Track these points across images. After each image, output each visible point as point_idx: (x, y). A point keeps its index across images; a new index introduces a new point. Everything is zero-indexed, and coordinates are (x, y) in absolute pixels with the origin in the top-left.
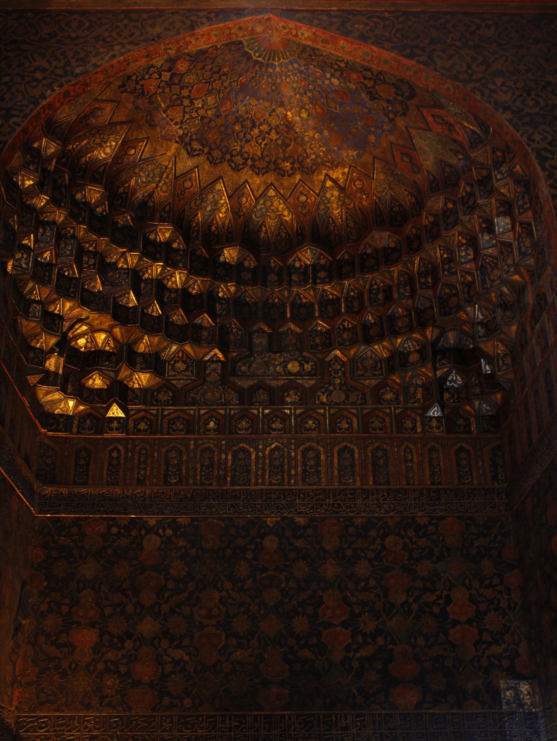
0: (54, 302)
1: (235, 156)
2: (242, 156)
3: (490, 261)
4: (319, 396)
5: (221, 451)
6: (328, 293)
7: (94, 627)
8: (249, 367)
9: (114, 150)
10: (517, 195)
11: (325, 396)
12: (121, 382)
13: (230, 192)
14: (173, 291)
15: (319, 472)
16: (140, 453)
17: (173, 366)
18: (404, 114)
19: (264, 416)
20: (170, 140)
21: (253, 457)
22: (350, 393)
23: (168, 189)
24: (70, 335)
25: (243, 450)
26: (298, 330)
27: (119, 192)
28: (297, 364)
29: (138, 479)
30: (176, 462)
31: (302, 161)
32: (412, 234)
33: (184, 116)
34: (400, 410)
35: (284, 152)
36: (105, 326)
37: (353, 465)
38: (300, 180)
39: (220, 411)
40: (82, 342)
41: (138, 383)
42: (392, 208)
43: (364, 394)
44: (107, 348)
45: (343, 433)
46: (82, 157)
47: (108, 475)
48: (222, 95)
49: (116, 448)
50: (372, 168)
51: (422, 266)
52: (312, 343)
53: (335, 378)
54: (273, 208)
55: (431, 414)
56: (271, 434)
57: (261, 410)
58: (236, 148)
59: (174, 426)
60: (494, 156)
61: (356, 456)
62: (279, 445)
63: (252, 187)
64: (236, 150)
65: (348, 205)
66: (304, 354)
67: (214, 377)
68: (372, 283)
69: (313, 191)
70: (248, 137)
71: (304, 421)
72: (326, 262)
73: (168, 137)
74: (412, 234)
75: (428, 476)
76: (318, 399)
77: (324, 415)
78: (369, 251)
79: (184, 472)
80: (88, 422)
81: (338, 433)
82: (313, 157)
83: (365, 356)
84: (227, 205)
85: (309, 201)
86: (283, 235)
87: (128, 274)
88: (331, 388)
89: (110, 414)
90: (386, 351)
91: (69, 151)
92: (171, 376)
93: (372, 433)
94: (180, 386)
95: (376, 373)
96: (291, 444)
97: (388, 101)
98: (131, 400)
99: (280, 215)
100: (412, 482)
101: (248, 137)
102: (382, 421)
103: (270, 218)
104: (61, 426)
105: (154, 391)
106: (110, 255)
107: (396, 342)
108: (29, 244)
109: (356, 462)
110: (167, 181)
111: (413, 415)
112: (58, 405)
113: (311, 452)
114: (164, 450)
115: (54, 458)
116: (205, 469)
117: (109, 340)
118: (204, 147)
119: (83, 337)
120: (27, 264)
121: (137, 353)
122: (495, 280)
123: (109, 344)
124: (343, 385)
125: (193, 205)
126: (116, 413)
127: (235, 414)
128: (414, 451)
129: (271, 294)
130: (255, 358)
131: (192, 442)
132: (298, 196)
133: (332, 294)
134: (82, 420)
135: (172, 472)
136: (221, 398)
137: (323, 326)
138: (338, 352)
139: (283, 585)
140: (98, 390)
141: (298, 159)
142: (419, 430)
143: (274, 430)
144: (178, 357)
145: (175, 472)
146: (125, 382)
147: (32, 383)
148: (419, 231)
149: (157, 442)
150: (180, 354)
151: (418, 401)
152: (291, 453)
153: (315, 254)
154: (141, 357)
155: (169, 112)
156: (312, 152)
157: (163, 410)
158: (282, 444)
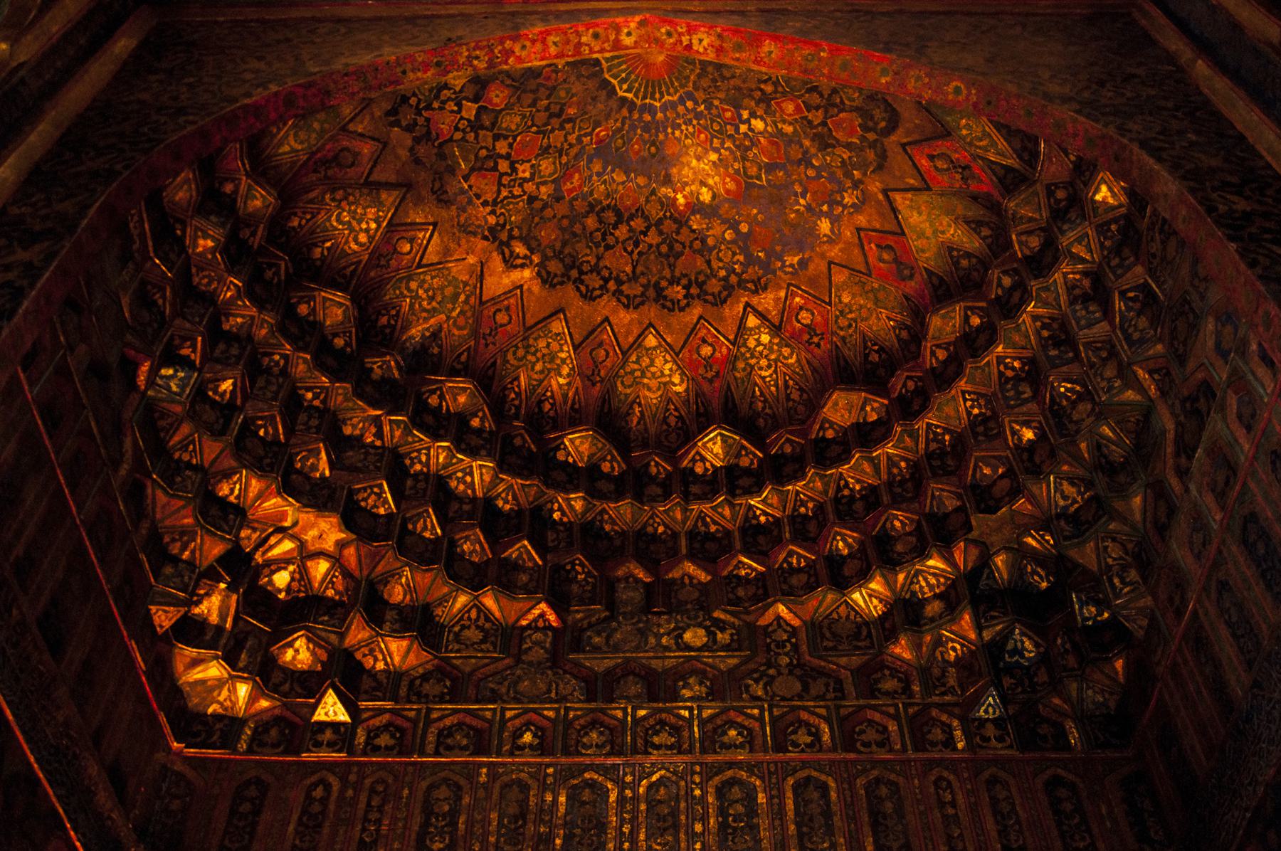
0: (227, 475)
1: (586, 273)
2: (599, 274)
3: (1067, 390)
4: (747, 687)
5: (544, 787)
6: (758, 512)
8: (608, 638)
9: (373, 238)
10: (1105, 253)
11: (760, 686)
12: (349, 654)
13: (578, 339)
14: (467, 501)
15: (753, 828)
16: (372, 791)
17: (457, 635)
18: (880, 167)
19: (636, 721)
20: (474, 234)
21: (613, 797)
22: (810, 680)
23: (467, 323)
24: (258, 558)
25: (592, 785)
26: (703, 577)
27: (380, 324)
28: (702, 632)
29: (361, 841)
30: (447, 808)
31: (704, 283)
32: (907, 391)
33: (499, 192)
34: (916, 708)
35: (672, 267)
36: (329, 544)
37: (827, 814)
38: (701, 317)
39: (546, 712)
40: (282, 579)
41: (384, 659)
42: (867, 356)
43: (839, 682)
44: (330, 593)
45: (803, 751)
46: (316, 245)
47: (297, 832)
48: (564, 160)
49: (322, 781)
50: (827, 284)
51: (933, 440)
52: (731, 596)
53: (780, 654)
54: (653, 369)
55: (982, 713)
56: (651, 754)
57: (629, 710)
58: (589, 258)
59: (449, 741)
60: (1052, 200)
61: (833, 795)
62: (668, 775)
63: (616, 330)
64: (588, 262)
65: (786, 358)
66: (717, 614)
67: (538, 654)
68: (839, 485)
69: (724, 337)
70: (611, 240)
71: (720, 731)
72: (752, 463)
73: (469, 229)
74: (907, 391)
75: (994, 834)
76: (747, 691)
77: (760, 719)
78: (830, 434)
79: (461, 826)
80: (274, 732)
81: (790, 752)
82: (723, 273)
83: (835, 616)
84: (572, 363)
85: (718, 355)
86: (672, 421)
87: (382, 455)
88: (772, 672)
89: (320, 715)
90: (874, 601)
91: (294, 228)
92: (451, 651)
93: (862, 752)
94: (468, 669)
95: (860, 644)
96: (694, 773)
97: (849, 146)
98: (366, 692)
99: (665, 384)
101: (611, 240)
102: (881, 729)
103: (649, 389)
104: (215, 738)
105: (416, 678)
106: (351, 419)
107: (896, 581)
108: (193, 356)
109: (835, 808)
110: (467, 308)
111: (944, 718)
112: (215, 694)
113: (736, 789)
114: (424, 784)
115: (188, 799)
116: (509, 822)
117: (334, 576)
118: (532, 253)
119: (285, 569)
120: (183, 388)
121: (387, 603)
122: (1083, 420)
123: (333, 583)
124: (795, 667)
125: (510, 356)
126: (331, 713)
127: (577, 718)
128: (956, 785)
129: (651, 517)
130: (619, 623)
131: (485, 770)
132: (699, 347)
133: (765, 513)
134: (260, 729)
135: (436, 828)
136: (549, 691)
137: (750, 567)
138: (782, 609)
140: (303, 672)
141: (696, 279)
142: (960, 745)
143: (658, 747)
144: (469, 619)
145: (443, 827)
146: (358, 656)
147: (161, 627)
148: (920, 384)
149: (410, 769)
150: (474, 614)
151: (951, 691)
152: (692, 790)
153: (730, 447)
154: (394, 612)
155: (472, 180)
156: (721, 265)
157: (429, 711)
158: (675, 773)
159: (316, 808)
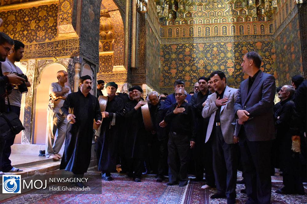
7: (175, 69)
28: (220, 5)
49: (178, 28)
100: (249, 33)
111: (250, 17)
139: (218, 59)
159: (178, 31)
